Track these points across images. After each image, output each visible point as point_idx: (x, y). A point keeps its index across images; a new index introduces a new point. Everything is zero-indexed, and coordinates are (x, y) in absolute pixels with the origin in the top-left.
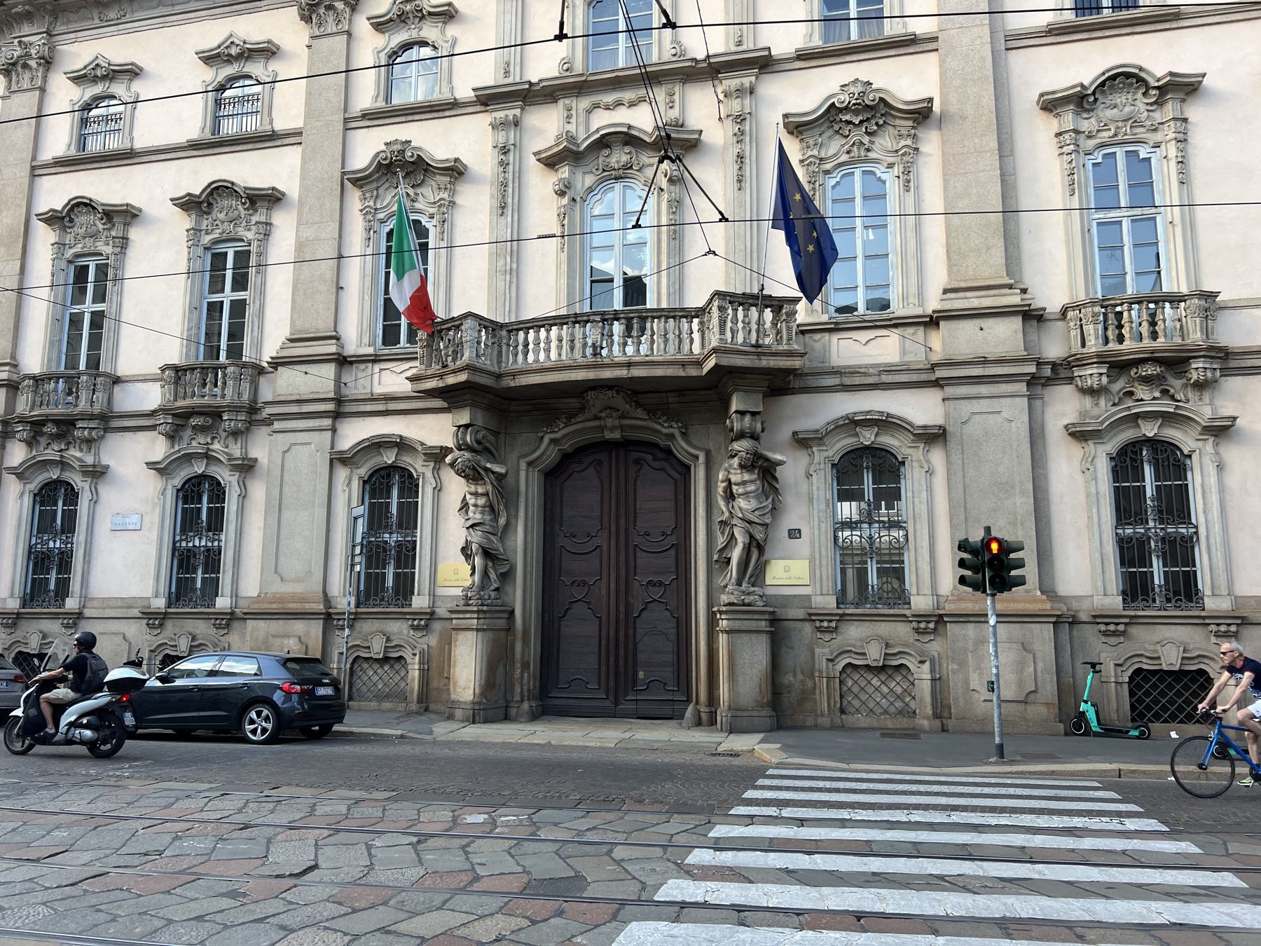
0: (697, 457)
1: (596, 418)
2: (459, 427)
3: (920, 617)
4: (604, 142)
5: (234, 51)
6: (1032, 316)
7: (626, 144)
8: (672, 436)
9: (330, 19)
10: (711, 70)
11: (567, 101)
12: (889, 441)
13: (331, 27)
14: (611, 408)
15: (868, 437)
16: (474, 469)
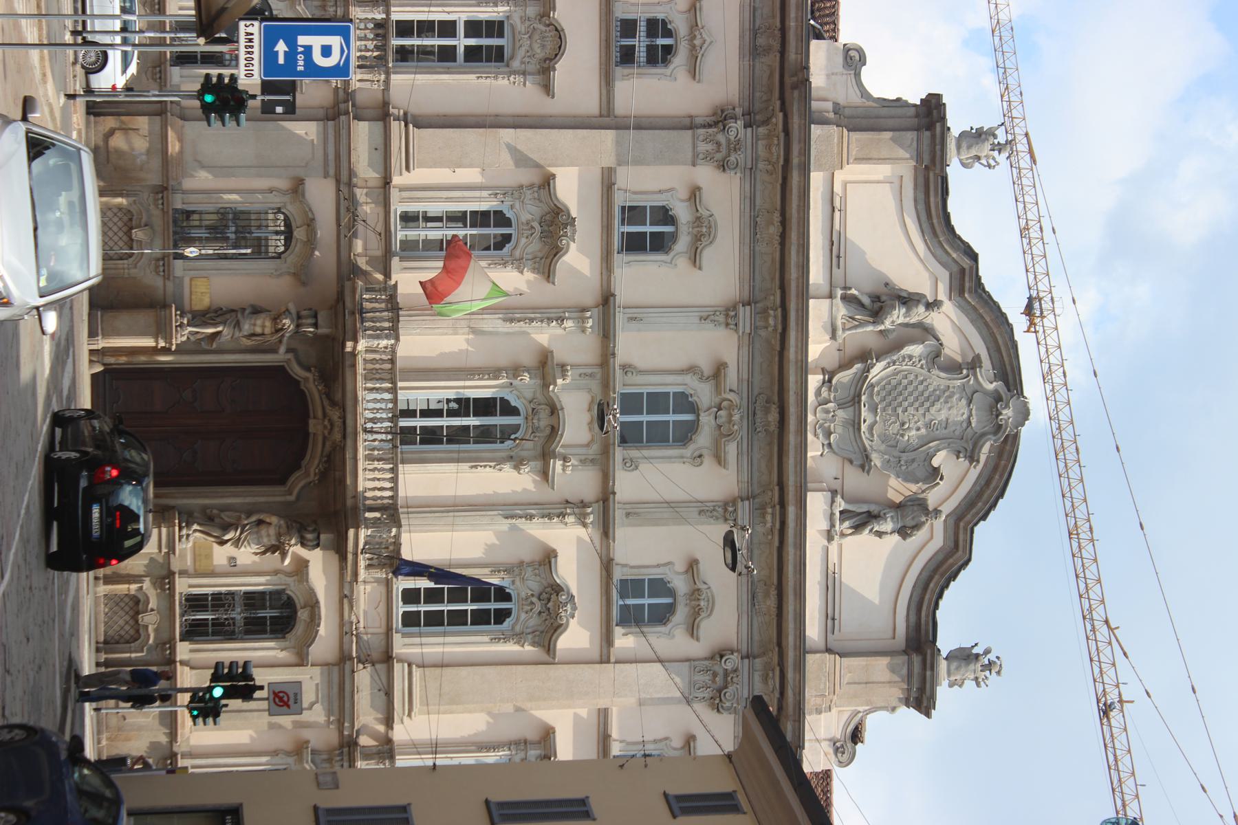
0: (291, 494)
1: (325, 415)
2: (315, 316)
3: (173, 649)
4: (554, 410)
5: (697, 42)
6: (389, 721)
7: (553, 428)
8: (307, 474)
9: (709, 147)
10: (606, 497)
11: (599, 376)
12: (299, 629)
13: (703, 147)
14: (331, 429)
15: (303, 615)
16: (282, 329)
